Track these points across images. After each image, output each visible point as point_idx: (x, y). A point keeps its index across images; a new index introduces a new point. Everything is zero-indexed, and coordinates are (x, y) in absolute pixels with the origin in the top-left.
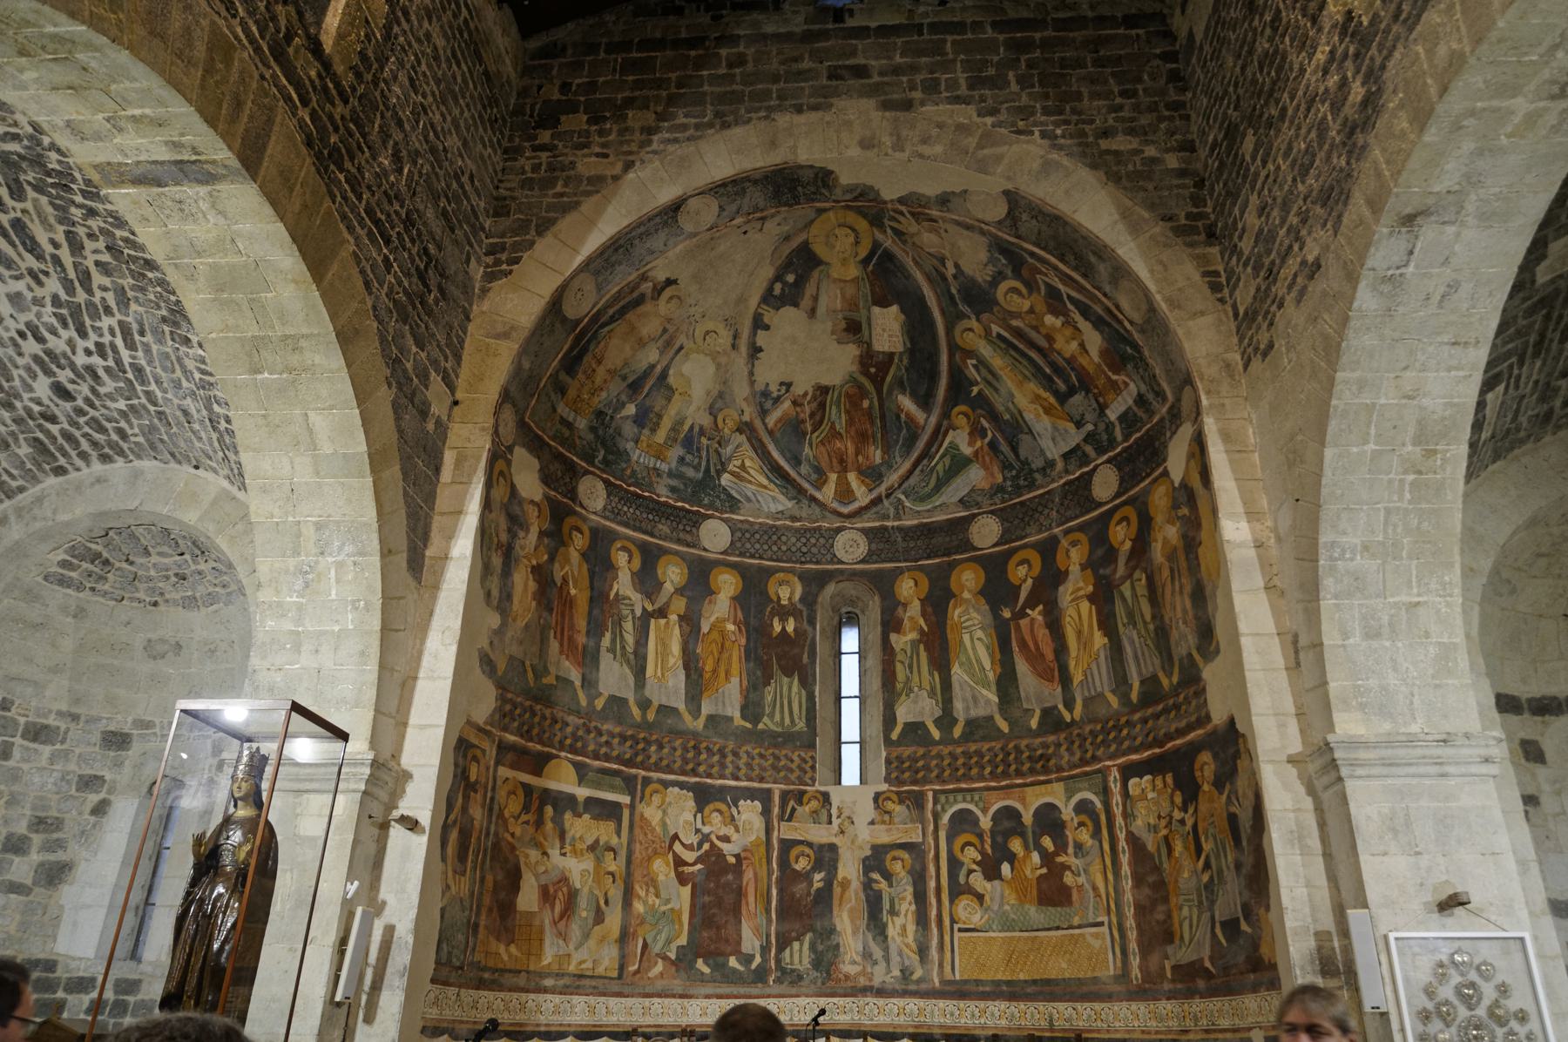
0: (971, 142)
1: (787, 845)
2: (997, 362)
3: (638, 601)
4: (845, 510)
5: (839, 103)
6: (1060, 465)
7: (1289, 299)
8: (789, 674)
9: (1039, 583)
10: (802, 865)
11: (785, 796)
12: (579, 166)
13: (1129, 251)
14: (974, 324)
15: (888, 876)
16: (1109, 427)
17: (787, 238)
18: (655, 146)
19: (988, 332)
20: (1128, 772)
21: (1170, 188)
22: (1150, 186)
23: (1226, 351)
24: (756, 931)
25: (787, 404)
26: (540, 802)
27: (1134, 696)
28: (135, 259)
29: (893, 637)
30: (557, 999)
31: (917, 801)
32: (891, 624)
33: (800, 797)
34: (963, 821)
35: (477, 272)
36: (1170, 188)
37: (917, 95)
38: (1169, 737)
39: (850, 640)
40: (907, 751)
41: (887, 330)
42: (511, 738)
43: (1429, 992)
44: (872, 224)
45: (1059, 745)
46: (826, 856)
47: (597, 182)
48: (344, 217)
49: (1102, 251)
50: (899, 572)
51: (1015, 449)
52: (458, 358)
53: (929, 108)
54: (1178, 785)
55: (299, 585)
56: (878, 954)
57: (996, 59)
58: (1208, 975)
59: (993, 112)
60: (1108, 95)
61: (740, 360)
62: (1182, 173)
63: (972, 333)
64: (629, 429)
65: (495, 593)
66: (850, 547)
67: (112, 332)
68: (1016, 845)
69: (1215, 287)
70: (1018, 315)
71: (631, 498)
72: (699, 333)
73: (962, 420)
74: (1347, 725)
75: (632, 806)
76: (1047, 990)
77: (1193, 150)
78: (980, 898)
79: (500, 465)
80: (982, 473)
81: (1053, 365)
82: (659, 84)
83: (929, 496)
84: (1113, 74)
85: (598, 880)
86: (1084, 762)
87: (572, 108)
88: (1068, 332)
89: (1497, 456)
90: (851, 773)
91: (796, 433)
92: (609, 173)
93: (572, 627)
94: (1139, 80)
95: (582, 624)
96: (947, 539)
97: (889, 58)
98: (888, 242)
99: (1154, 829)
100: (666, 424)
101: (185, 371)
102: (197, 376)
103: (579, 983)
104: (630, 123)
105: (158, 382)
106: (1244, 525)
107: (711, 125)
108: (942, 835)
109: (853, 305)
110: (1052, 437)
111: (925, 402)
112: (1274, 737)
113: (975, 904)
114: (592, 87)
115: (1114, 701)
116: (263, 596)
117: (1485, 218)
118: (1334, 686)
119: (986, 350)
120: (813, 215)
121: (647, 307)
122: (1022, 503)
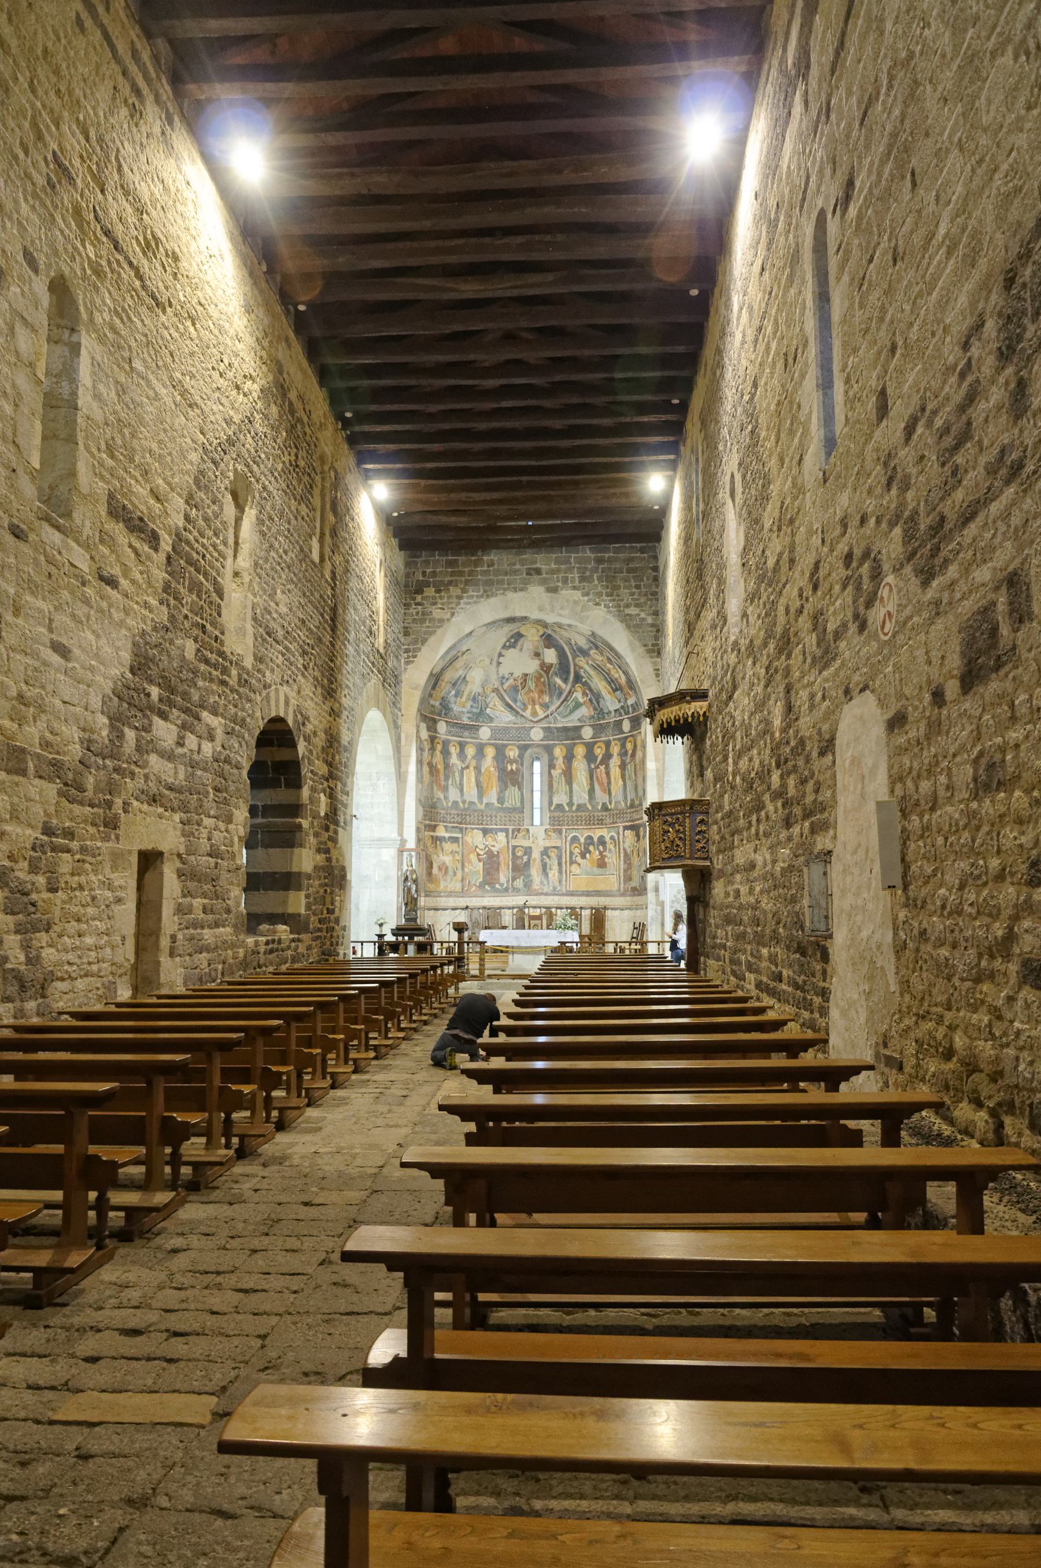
1: (514, 847)
10: (520, 854)
20: (626, 828)
25: (511, 681)
31: (560, 832)
32: (552, 766)
33: (519, 830)
34: (575, 839)
39: (537, 765)
40: (556, 814)
41: (550, 656)
46: (528, 851)
53: (563, 592)
59: (587, 594)
61: (494, 668)
62: (652, 625)
63: (582, 661)
64: (452, 700)
66: (537, 735)
68: (591, 848)
69: (657, 675)
76: (598, 893)
82: (461, 574)
90: (537, 821)
91: (513, 692)
95: (442, 777)
96: (572, 733)
100: (466, 694)
103: (451, 894)
110: (611, 703)
111: (565, 681)
114: (434, 574)
119: (588, 668)
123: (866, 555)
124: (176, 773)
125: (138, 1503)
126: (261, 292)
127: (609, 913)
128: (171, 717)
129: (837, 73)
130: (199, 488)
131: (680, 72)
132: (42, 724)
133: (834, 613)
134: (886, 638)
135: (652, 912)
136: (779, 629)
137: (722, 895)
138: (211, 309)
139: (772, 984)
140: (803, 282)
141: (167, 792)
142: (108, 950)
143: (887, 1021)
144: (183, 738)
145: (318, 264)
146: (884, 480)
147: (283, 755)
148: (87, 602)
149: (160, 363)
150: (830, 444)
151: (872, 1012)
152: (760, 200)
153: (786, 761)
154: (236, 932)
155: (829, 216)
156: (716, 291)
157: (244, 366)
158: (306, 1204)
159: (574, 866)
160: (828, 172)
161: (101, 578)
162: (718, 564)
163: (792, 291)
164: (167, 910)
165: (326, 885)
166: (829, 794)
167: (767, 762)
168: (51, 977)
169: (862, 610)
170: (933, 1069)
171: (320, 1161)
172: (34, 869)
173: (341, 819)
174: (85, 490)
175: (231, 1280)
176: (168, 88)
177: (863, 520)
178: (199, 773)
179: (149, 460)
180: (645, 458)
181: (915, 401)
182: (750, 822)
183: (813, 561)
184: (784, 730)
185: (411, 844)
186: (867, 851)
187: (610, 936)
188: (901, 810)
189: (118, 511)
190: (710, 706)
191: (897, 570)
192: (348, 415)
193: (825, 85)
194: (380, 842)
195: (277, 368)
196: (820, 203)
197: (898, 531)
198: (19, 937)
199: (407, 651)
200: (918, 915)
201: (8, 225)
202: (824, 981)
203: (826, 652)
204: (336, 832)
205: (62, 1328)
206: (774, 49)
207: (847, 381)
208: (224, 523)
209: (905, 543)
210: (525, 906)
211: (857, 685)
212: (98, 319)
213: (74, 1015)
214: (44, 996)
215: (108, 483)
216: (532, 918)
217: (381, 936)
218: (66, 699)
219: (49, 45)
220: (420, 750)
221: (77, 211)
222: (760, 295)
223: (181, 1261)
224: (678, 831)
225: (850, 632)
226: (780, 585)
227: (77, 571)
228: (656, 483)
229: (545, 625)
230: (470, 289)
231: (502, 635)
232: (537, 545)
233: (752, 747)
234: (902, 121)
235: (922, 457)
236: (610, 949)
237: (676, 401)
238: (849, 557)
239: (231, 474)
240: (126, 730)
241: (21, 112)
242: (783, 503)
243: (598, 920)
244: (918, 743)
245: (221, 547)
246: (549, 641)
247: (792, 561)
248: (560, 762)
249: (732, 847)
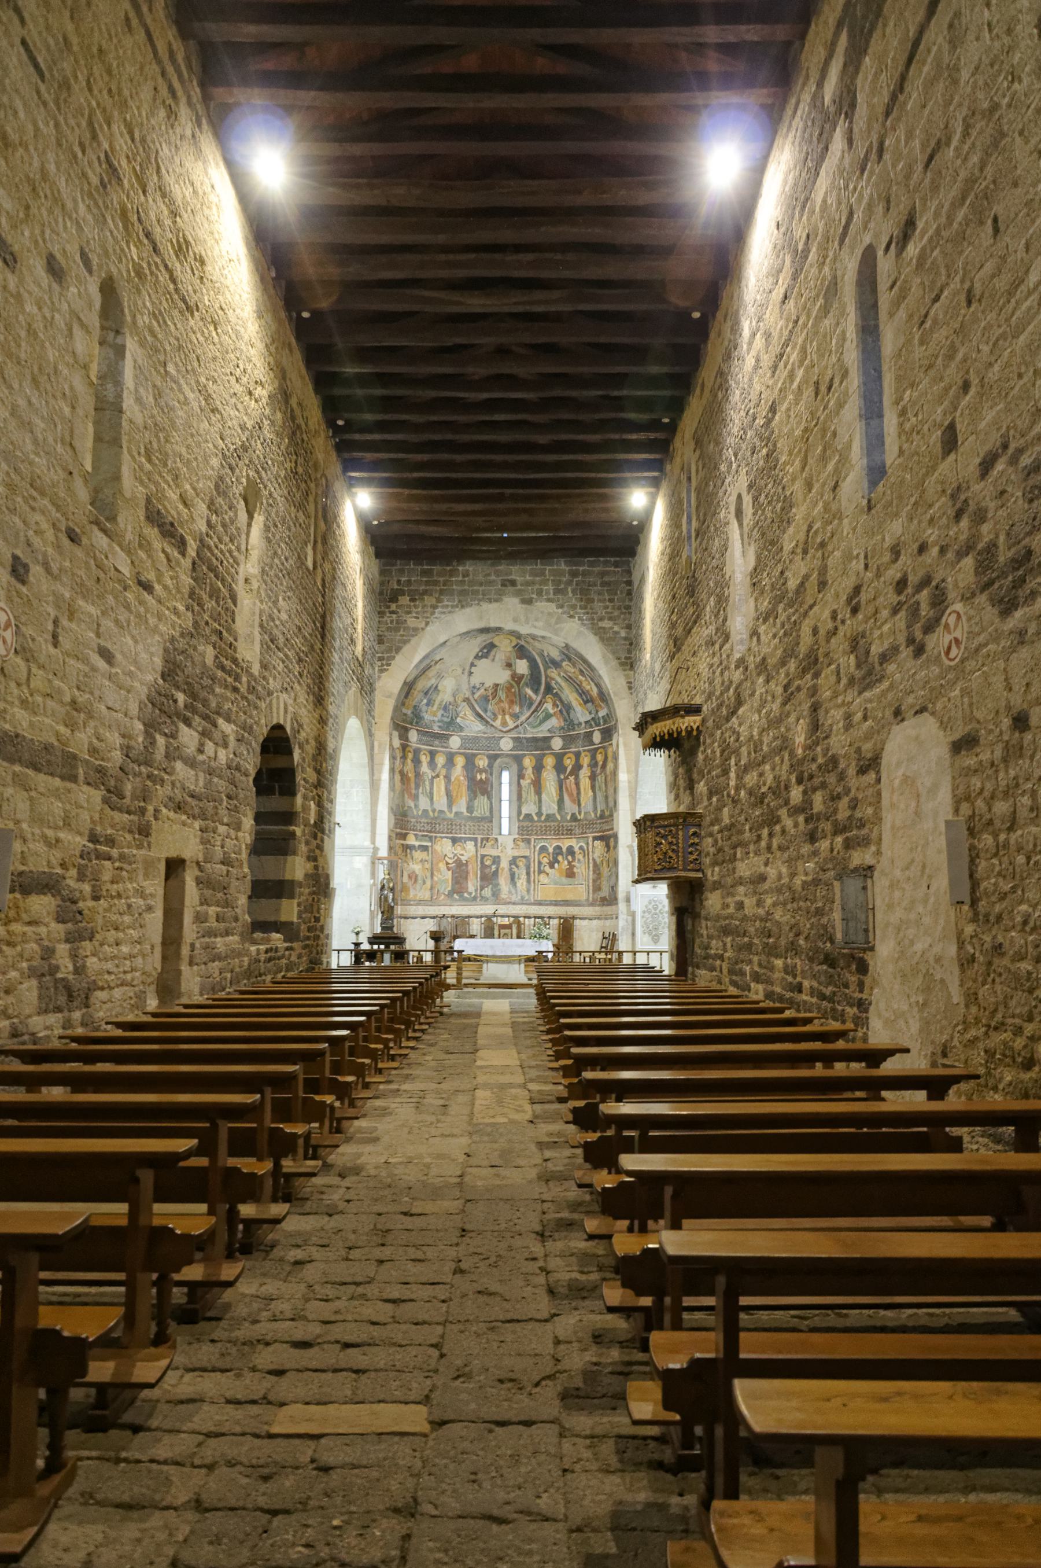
0: (553, 621)
1: (483, 856)
5: (506, 599)
10: (488, 863)
20: (595, 838)
25: (482, 691)
26: (407, 848)
31: (528, 841)
32: (521, 776)
33: (487, 839)
34: (543, 849)
39: (506, 776)
40: (525, 824)
41: (522, 667)
46: (496, 860)
47: (416, 630)
59: (562, 607)
61: (465, 677)
62: (626, 639)
63: (553, 673)
64: (424, 708)
66: (506, 744)
68: (560, 858)
69: (630, 688)
71: (428, 735)
76: (566, 903)
90: (505, 830)
91: (483, 702)
95: (413, 785)
96: (542, 744)
98: (523, 643)
103: (420, 902)
110: (581, 714)
111: (536, 691)
119: (559, 680)
123: (926, 581)
124: (197, 780)
125: (409, 1510)
126: (270, 297)
127: (577, 922)
128: (194, 724)
129: (894, 115)
130: (219, 494)
131: (700, 102)
132: (90, 731)
133: (881, 636)
134: (952, 663)
135: (622, 922)
136: (803, 649)
137: (719, 906)
138: (230, 313)
139: (788, 995)
140: (843, 313)
141: (189, 799)
142: (140, 960)
143: (949, 1031)
144: (202, 745)
145: (334, 272)
146: (951, 512)
147: (279, 762)
148: (127, 607)
149: (189, 368)
150: (876, 473)
151: (926, 1023)
152: (782, 229)
153: (811, 777)
154: (243, 939)
155: (880, 253)
156: (719, 315)
157: (256, 372)
158: (405, 1214)
159: (542, 876)
160: (880, 209)
161: (140, 583)
162: (716, 584)
163: (827, 322)
164: (188, 918)
165: (314, 893)
166: (870, 811)
167: (784, 778)
168: (94, 987)
169: (918, 635)
170: (1009, 1078)
171: (396, 1172)
172: (81, 877)
173: (327, 827)
174: (128, 494)
175: (372, 1291)
176: (198, 90)
177: (922, 549)
178: (216, 780)
179: (179, 465)
180: (628, 475)
181: (994, 440)
182: (759, 837)
183: (852, 586)
184: (808, 747)
185: (383, 852)
186: (924, 867)
187: (578, 946)
188: (969, 829)
189: (155, 517)
190: (704, 721)
191: (968, 597)
192: (340, 423)
193: (876, 126)
194: (354, 850)
195: (280, 372)
196: (867, 240)
197: (968, 562)
198: (68, 946)
199: (380, 659)
200: (990, 930)
201: (69, 224)
202: (861, 991)
203: (870, 673)
204: (322, 841)
205: (229, 1342)
206: (804, 84)
207: (903, 413)
208: (238, 529)
209: (977, 573)
210: (494, 915)
211: (912, 706)
212: (140, 323)
213: (118, 1025)
214: (87, 1006)
215: (146, 487)
216: (502, 927)
217: (357, 945)
218: (110, 704)
219: (104, 42)
220: (393, 758)
221: (124, 214)
222: (781, 323)
223: (310, 1273)
224: (671, 843)
225: (903, 655)
226: (806, 607)
227: (121, 576)
228: (640, 499)
229: (518, 636)
230: (475, 303)
231: (475, 645)
232: (513, 557)
233: (763, 762)
234: (981, 170)
235: (1003, 492)
236: (577, 958)
237: (666, 420)
238: (901, 585)
239: (244, 480)
240: (158, 736)
241: (79, 111)
242: (810, 527)
243: (566, 930)
244: (992, 764)
245: (236, 554)
246: (521, 652)
247: (822, 585)
248: (529, 772)
249: (734, 859)
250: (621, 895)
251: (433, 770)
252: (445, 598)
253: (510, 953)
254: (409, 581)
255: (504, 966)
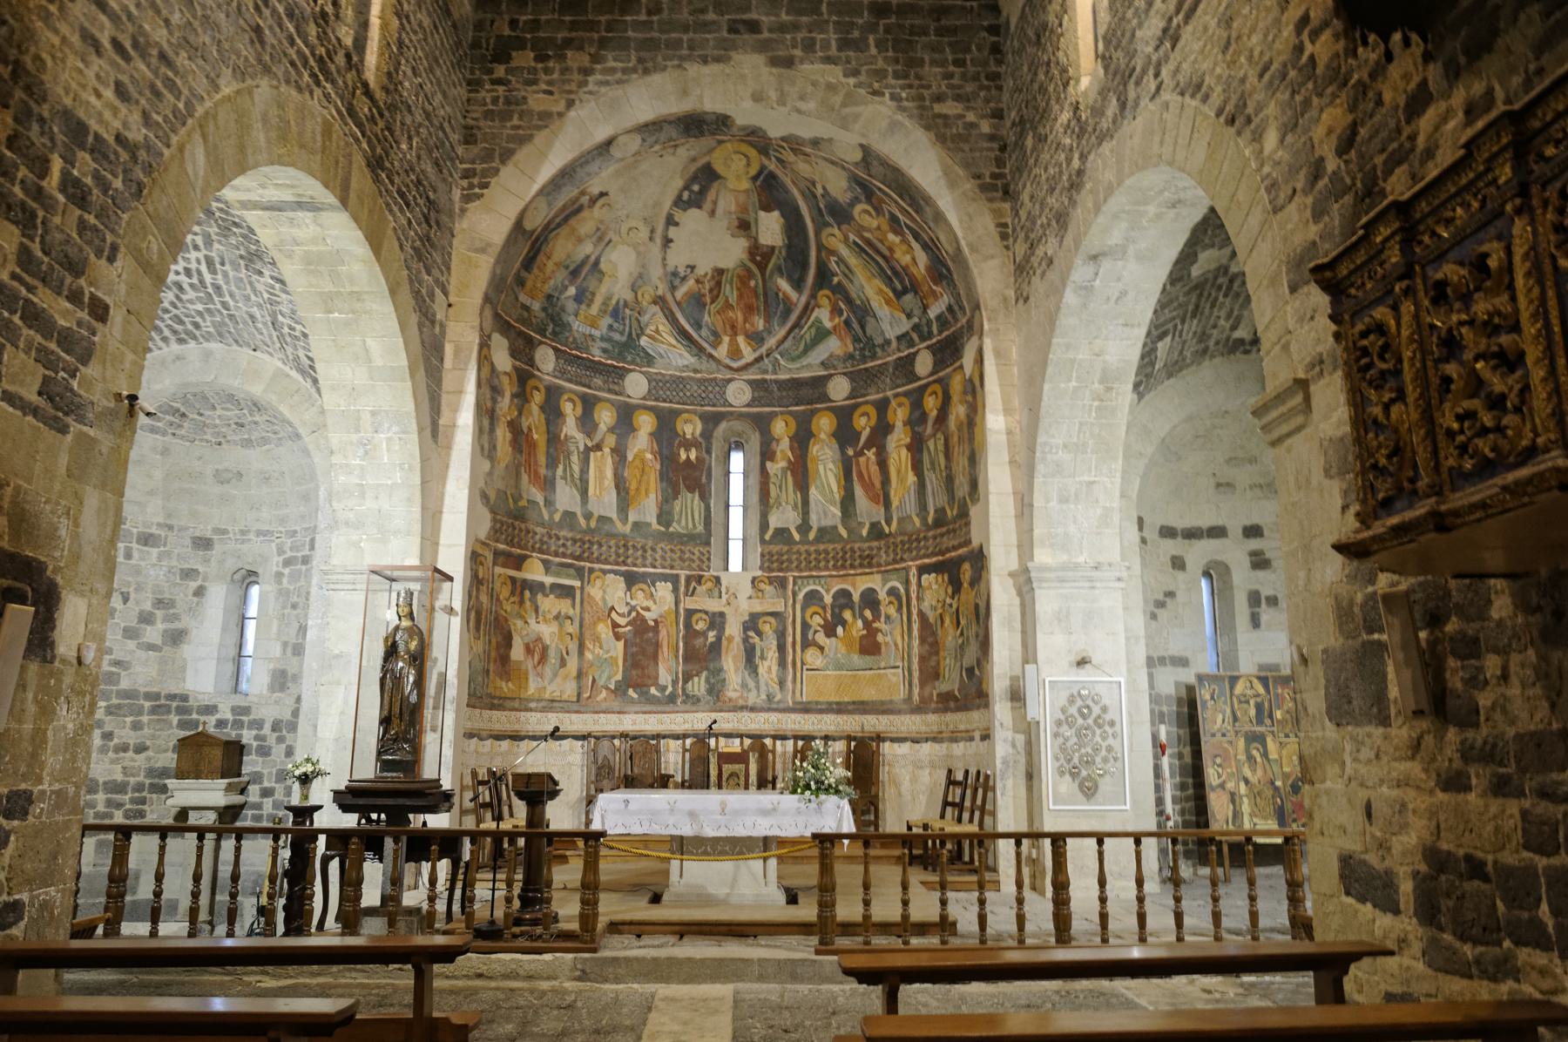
0: (837, 100)
1: (690, 613)
2: (853, 261)
3: (581, 440)
4: (735, 365)
5: (737, 57)
6: (894, 344)
7: (1038, 272)
8: (691, 489)
9: (874, 431)
10: (700, 626)
11: (688, 579)
12: (530, 101)
13: (946, 202)
14: (836, 231)
15: (759, 634)
16: (929, 322)
17: (694, 160)
18: (591, 87)
19: (846, 238)
20: (923, 570)
21: (981, 150)
22: (966, 147)
23: (1007, 287)
24: (669, 670)
25: (691, 282)
26: (523, 589)
27: (930, 520)
28: (223, 220)
29: (769, 464)
30: (539, 715)
31: (782, 583)
32: (767, 455)
33: (699, 579)
34: (813, 597)
35: (457, 194)
36: (981, 150)
37: (798, 52)
38: (948, 550)
39: (737, 460)
40: (775, 548)
41: (771, 229)
42: (502, 546)
43: (1063, 711)
44: (760, 152)
45: (879, 549)
46: (717, 621)
47: (546, 116)
48: (388, 205)
49: (928, 200)
50: (773, 415)
51: (863, 327)
52: (449, 269)
53: (806, 67)
54: (951, 582)
55: (361, 452)
56: (751, 684)
57: (860, 21)
58: (956, 699)
60: (942, 63)
61: (656, 248)
63: (834, 238)
64: (571, 306)
65: (486, 446)
66: (738, 394)
67: (198, 262)
68: (847, 615)
69: (1004, 236)
70: (869, 230)
71: (575, 361)
72: (624, 229)
73: (825, 301)
74: (1042, 556)
75: (582, 588)
76: (862, 707)
77: (1001, 117)
78: (822, 649)
79: (485, 351)
80: (839, 343)
81: (892, 268)
82: (592, 26)
83: (799, 357)
84: (950, 44)
85: (561, 638)
86: (895, 561)
87: (520, 45)
88: (904, 247)
89: (1170, 375)
90: (735, 564)
91: (696, 305)
92: (555, 109)
93: (536, 463)
94: (968, 50)
95: (542, 459)
96: (810, 391)
97: (777, 15)
98: (772, 166)
99: (935, 609)
100: (599, 300)
101: (254, 290)
102: (266, 296)
103: (551, 705)
104: (569, 63)
105: (231, 295)
106: (1001, 418)
107: (634, 70)
108: (798, 607)
109: (744, 209)
110: (890, 322)
111: (798, 285)
112: (1001, 560)
113: (818, 652)
114: (535, 25)
115: (917, 521)
116: (335, 459)
117: (1140, 258)
118: (1036, 532)
119: (844, 252)
120: (714, 143)
121: (585, 213)
122: (866, 370)
127: (887, 748)
135: (1005, 745)
199: (467, 175)
210: (710, 732)
216: (726, 758)
248: (784, 447)
250: (999, 684)
251: (589, 435)
252: (610, 56)
253: (740, 832)
254: (536, 21)
255: (726, 867)
